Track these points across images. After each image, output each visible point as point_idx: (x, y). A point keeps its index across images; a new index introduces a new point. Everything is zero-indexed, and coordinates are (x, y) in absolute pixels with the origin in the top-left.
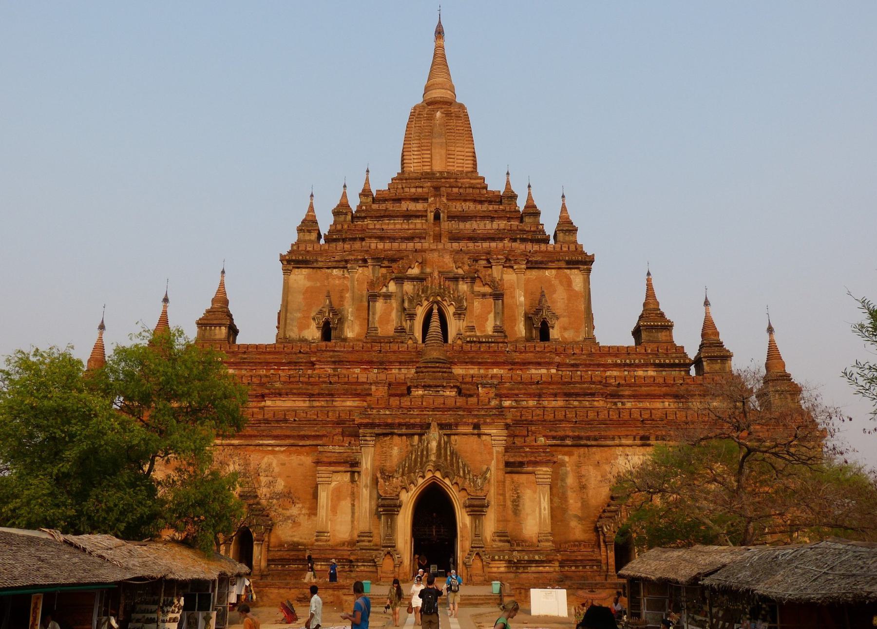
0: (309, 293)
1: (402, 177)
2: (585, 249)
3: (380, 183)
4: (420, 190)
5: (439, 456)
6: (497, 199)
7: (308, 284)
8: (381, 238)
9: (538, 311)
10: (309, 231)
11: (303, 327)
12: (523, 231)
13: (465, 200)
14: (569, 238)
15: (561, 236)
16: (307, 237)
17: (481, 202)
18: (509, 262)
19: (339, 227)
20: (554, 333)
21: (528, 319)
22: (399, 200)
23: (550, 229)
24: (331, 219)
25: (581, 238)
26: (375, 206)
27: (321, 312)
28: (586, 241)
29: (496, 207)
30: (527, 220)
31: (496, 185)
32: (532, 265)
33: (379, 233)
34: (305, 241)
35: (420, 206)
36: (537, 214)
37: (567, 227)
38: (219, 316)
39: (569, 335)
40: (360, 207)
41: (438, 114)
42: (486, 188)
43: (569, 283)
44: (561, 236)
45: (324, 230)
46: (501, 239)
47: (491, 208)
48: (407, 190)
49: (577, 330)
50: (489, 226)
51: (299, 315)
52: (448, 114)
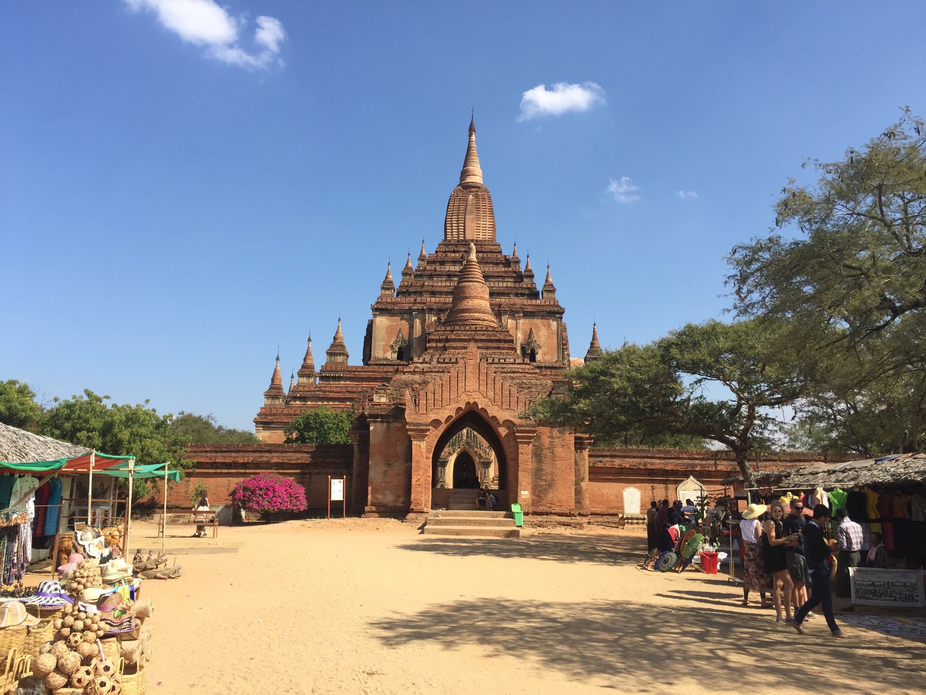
0: (389, 329)
1: (446, 243)
2: (560, 304)
3: (430, 250)
4: (457, 255)
5: (467, 437)
6: (507, 263)
7: (389, 324)
8: (433, 293)
9: (528, 344)
10: (388, 289)
11: (384, 352)
12: (523, 288)
13: (487, 263)
14: (550, 295)
15: (545, 294)
16: (388, 292)
17: (497, 264)
18: (513, 313)
19: (406, 284)
20: (539, 357)
21: (523, 349)
22: (442, 263)
23: (540, 287)
24: (401, 278)
25: (558, 296)
26: (428, 268)
27: (396, 342)
28: (562, 298)
29: (506, 269)
30: (525, 280)
31: (507, 252)
32: (528, 315)
33: (430, 289)
34: (386, 296)
35: (457, 268)
36: (532, 276)
37: (550, 289)
38: (337, 349)
39: (547, 358)
40: (419, 267)
41: (471, 196)
42: (501, 252)
43: (549, 326)
44: (545, 294)
45: (397, 285)
46: (508, 294)
47: (503, 269)
48: (449, 254)
49: (553, 355)
50: (501, 285)
51: (383, 343)
52: (477, 197)
